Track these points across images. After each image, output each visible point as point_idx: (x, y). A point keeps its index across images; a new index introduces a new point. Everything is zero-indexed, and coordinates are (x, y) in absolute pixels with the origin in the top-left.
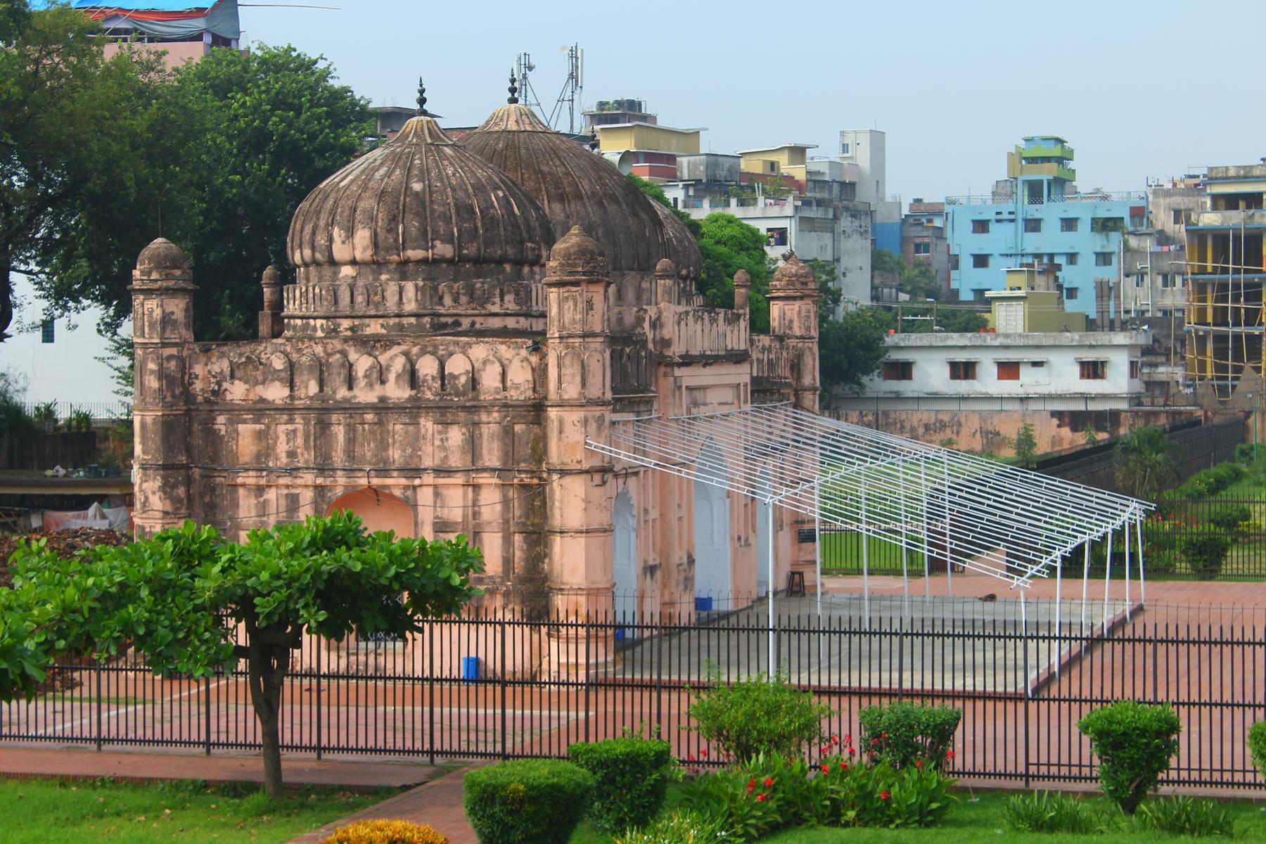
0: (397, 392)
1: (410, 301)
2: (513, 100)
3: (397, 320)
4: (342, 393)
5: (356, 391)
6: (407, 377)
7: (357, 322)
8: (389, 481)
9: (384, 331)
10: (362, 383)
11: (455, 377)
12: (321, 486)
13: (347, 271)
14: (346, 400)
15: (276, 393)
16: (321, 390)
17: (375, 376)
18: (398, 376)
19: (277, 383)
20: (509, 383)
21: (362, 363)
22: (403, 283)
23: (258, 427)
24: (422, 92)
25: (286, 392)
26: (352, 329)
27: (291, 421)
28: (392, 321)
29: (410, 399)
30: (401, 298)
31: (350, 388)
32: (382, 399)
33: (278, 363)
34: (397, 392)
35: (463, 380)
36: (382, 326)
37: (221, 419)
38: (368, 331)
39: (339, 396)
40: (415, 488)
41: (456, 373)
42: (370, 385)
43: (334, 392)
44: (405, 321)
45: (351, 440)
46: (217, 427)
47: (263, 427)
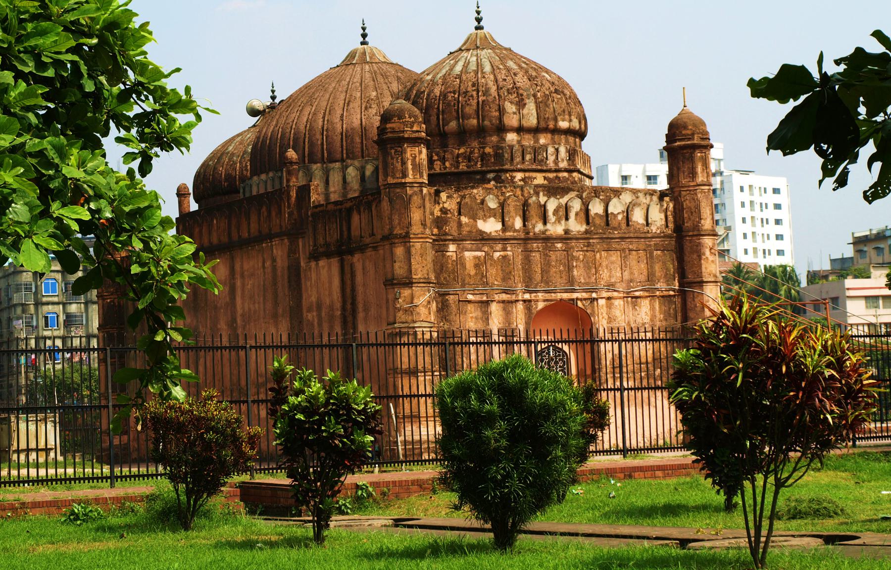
0: (576, 226)
1: (563, 160)
2: (363, 43)
3: (555, 174)
4: (539, 227)
5: (549, 226)
6: (582, 215)
7: (527, 174)
9: (546, 182)
10: (552, 218)
11: (615, 216)
12: (530, 301)
13: (511, 137)
14: (544, 232)
15: (491, 226)
16: (524, 225)
17: (562, 213)
18: (577, 214)
19: (492, 219)
20: (650, 221)
21: (552, 205)
23: (479, 254)
25: (499, 226)
26: (523, 180)
27: (504, 249)
28: (551, 175)
29: (586, 232)
31: (545, 223)
32: (567, 232)
33: (492, 204)
34: (576, 226)
35: (620, 217)
36: (545, 178)
37: (452, 247)
38: (536, 182)
39: (537, 230)
40: (593, 300)
41: (616, 213)
42: (559, 220)
43: (534, 228)
44: (561, 175)
46: (448, 254)
47: (483, 253)
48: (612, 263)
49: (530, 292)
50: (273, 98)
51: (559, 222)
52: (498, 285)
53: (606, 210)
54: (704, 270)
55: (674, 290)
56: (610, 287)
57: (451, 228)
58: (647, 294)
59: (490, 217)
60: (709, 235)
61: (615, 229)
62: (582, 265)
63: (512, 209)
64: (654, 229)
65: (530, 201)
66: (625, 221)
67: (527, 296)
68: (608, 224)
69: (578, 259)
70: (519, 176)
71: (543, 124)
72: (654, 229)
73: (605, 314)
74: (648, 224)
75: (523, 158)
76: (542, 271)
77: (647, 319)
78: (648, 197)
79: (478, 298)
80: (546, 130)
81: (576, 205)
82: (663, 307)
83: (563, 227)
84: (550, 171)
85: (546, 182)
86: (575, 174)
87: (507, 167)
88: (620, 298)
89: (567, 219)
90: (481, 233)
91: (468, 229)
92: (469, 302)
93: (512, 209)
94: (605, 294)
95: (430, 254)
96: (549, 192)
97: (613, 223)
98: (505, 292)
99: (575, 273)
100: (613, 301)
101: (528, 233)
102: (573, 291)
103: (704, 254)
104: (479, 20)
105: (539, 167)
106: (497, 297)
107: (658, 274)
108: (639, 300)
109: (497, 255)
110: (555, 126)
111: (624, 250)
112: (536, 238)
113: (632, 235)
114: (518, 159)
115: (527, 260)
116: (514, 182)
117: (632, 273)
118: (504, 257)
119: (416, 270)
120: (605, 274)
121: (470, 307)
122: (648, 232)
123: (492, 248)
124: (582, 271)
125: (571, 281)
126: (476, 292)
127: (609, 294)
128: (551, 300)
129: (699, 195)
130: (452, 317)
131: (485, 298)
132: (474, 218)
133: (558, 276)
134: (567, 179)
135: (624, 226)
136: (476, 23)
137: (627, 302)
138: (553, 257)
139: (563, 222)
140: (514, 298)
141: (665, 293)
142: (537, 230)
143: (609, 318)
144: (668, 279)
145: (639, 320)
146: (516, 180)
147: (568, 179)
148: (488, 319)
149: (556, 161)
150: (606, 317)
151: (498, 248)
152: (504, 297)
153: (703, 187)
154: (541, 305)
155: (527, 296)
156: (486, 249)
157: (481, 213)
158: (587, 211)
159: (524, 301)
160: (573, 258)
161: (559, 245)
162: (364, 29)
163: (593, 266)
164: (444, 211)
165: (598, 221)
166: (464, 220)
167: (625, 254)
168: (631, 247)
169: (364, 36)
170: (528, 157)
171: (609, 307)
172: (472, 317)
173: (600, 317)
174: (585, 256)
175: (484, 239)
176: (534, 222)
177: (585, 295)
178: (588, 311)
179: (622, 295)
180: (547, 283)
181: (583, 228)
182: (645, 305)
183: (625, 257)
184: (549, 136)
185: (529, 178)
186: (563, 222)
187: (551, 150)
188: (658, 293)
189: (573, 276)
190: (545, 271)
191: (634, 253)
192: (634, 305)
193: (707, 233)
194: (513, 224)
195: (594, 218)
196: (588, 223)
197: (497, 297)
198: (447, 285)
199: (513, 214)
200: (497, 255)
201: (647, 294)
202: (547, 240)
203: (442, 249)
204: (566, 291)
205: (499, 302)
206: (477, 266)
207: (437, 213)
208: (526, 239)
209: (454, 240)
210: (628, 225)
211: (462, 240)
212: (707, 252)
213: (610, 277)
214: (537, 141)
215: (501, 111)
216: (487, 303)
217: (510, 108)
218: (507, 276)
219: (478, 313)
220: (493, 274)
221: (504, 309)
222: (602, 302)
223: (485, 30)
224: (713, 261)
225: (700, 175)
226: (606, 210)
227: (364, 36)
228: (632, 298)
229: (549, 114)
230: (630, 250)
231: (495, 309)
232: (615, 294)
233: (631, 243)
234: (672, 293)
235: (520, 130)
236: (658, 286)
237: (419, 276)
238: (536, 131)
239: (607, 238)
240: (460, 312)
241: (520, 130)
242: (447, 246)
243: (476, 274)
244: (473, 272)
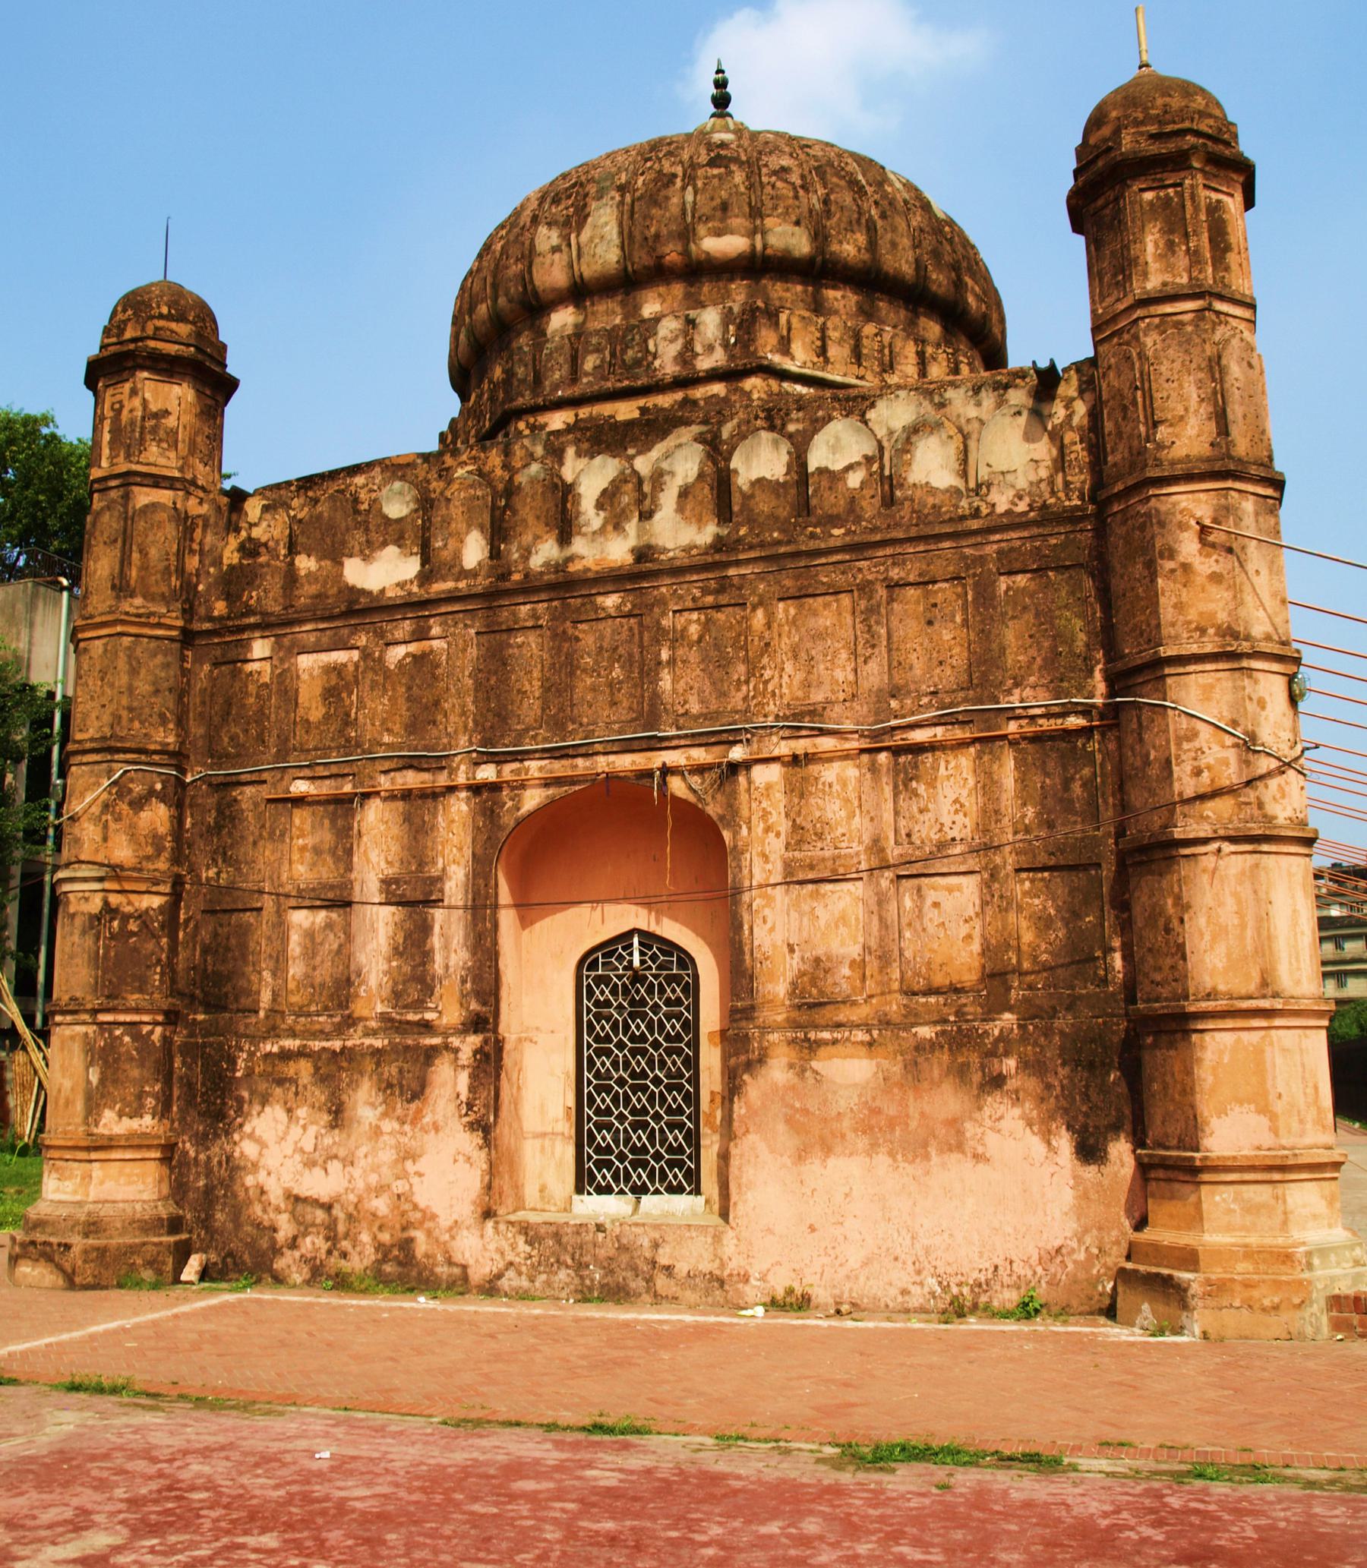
1: (710, 349)
3: (679, 396)
4: (546, 552)
6: (706, 492)
8: (659, 759)
11: (833, 477)
12: (495, 787)
14: (560, 567)
16: (495, 554)
18: (684, 493)
19: (392, 550)
22: (692, 314)
23: (340, 657)
24: (721, 84)
27: (421, 635)
29: (719, 545)
30: (689, 346)
31: (564, 538)
32: (643, 554)
34: (678, 532)
37: (260, 648)
39: (536, 562)
40: (734, 768)
41: (837, 466)
42: (616, 524)
43: (526, 554)
45: (564, 667)
47: (355, 655)
48: (819, 636)
49: (499, 759)
51: (618, 527)
52: (390, 746)
55: (1086, 711)
56: (804, 719)
57: (267, 596)
58: (959, 733)
59: (385, 544)
60: (1189, 477)
61: (834, 520)
62: (694, 656)
64: (1002, 500)
65: (521, 479)
67: (487, 773)
69: (678, 638)
71: (642, 259)
76: (546, 689)
77: (962, 827)
78: (988, 399)
79: (326, 788)
80: (658, 274)
82: (1037, 780)
83: (632, 541)
84: (658, 387)
86: (754, 384)
88: (846, 756)
89: (646, 516)
91: (312, 589)
92: (299, 801)
93: (456, 511)
94: (784, 748)
97: (829, 502)
98: (411, 764)
99: (666, 682)
100: (814, 769)
101: (504, 576)
103: (1171, 553)
106: (384, 782)
108: (928, 758)
109: (397, 653)
110: (686, 253)
112: (530, 587)
115: (496, 663)
117: (894, 665)
118: (419, 659)
119: (86, 716)
120: (785, 681)
121: (301, 818)
122: (976, 513)
123: (381, 634)
124: (693, 675)
125: (650, 712)
126: (321, 771)
127: (801, 746)
128: (571, 781)
130: (245, 850)
131: (348, 788)
132: (335, 554)
133: (603, 698)
135: (870, 507)
137: (873, 769)
140: (442, 779)
141: (1045, 724)
142: (536, 562)
143: (796, 828)
144: (1061, 671)
145: (926, 832)
148: (349, 852)
149: (686, 356)
150: (784, 826)
151: (399, 635)
152: (411, 779)
153: (1168, 309)
154: (533, 799)
156: (362, 640)
159: (476, 789)
160: (660, 635)
161: (611, 601)
164: (251, 548)
165: (764, 505)
166: (305, 564)
168: (895, 573)
170: (590, 363)
172: (303, 849)
173: (759, 828)
174: (707, 626)
175: (361, 610)
176: (527, 538)
177: (700, 755)
178: (713, 810)
179: (854, 744)
180: (558, 726)
183: (871, 611)
184: (678, 289)
186: (632, 526)
187: (669, 326)
188: (1012, 727)
189: (656, 696)
191: (911, 592)
192: (904, 782)
193: (1179, 470)
194: (457, 556)
195: (747, 497)
197: (384, 782)
198: (237, 758)
199: (458, 524)
200: (397, 653)
201: (959, 733)
202: (567, 586)
203: (232, 655)
204: (628, 747)
205: (392, 797)
207: (231, 556)
208: (498, 591)
209: (266, 626)
211: (291, 623)
212: (1188, 546)
213: (807, 685)
214: (632, 310)
216: (342, 807)
218: (423, 715)
219: (326, 836)
220: (378, 715)
221: (407, 818)
224: (1216, 578)
225: (1153, 266)
226: (798, 461)
228: (896, 751)
229: (662, 220)
230: (893, 586)
231: (377, 821)
232: (827, 743)
233: (897, 560)
234: (1074, 721)
235: (579, 292)
236: (1014, 700)
237: (91, 733)
238: (625, 283)
239: (796, 555)
240: (277, 836)
241: (579, 292)
242: (246, 645)
243: (327, 717)
244: (316, 714)
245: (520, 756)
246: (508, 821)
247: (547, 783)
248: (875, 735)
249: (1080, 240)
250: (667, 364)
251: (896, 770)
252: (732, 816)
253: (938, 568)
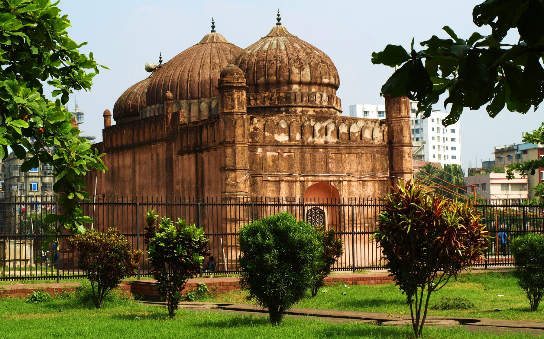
0: (331, 139)
1: (325, 101)
3: (320, 109)
4: (310, 139)
5: (316, 139)
6: (335, 133)
7: (304, 109)
8: (330, 179)
10: (317, 134)
11: (354, 134)
12: (304, 181)
13: (295, 87)
14: (313, 142)
15: (282, 138)
16: (302, 138)
17: (323, 131)
18: (332, 132)
19: (283, 134)
20: (374, 137)
21: (318, 127)
23: (275, 154)
25: (287, 138)
26: (301, 112)
27: (290, 152)
28: (318, 110)
29: (337, 143)
31: (313, 137)
32: (326, 142)
33: (283, 125)
34: (331, 139)
35: (357, 135)
36: (314, 111)
37: (260, 150)
38: (309, 113)
40: (340, 182)
41: (354, 132)
42: (321, 136)
43: (307, 139)
44: (323, 109)
46: (257, 153)
48: (352, 161)
49: (304, 176)
50: (161, 62)
51: (322, 137)
52: (285, 172)
53: (349, 130)
54: (404, 166)
55: (387, 177)
56: (350, 174)
57: (259, 139)
58: (371, 179)
59: (282, 133)
61: (354, 141)
62: (334, 162)
63: (294, 128)
64: (376, 142)
65: (305, 124)
66: (359, 137)
67: (302, 179)
68: (349, 138)
69: (332, 158)
70: (299, 110)
71: (314, 80)
72: (376, 142)
73: (346, 190)
74: (373, 139)
75: (302, 100)
76: (311, 165)
77: (371, 194)
78: (373, 124)
79: (274, 179)
80: (316, 84)
81: (332, 127)
82: (380, 187)
83: (324, 140)
84: (317, 107)
85: (315, 113)
86: (332, 109)
87: (292, 104)
89: (326, 135)
90: (277, 142)
91: (269, 139)
92: (269, 181)
93: (294, 128)
94: (347, 179)
95: (247, 153)
96: (316, 119)
97: (353, 138)
98: (290, 176)
99: (330, 166)
100: (352, 182)
101: (303, 143)
102: (329, 176)
103: (405, 157)
104: (279, 20)
105: (311, 105)
107: (378, 168)
108: (366, 182)
110: (321, 81)
111: (358, 153)
112: (308, 146)
113: (363, 145)
114: (299, 100)
115: (303, 158)
116: (296, 113)
117: (363, 167)
118: (289, 156)
119: (239, 162)
120: (347, 167)
121: (269, 184)
124: (334, 165)
125: (328, 170)
126: (273, 176)
128: (316, 181)
129: (403, 123)
130: (259, 190)
131: (278, 179)
132: (273, 133)
133: (320, 167)
134: (326, 112)
135: (359, 140)
136: (277, 22)
138: (318, 157)
139: (324, 137)
140: (294, 179)
141: (382, 179)
143: (349, 192)
144: (384, 171)
145: (366, 194)
146: (298, 112)
147: (327, 112)
148: (279, 191)
150: (347, 192)
151: (286, 151)
152: (289, 179)
154: (310, 184)
155: (302, 179)
156: (279, 151)
157: (277, 130)
158: (338, 131)
159: (301, 181)
160: (329, 157)
161: (321, 150)
162: (213, 23)
163: (340, 162)
164: (255, 129)
165: (344, 137)
166: (267, 134)
167: (359, 156)
169: (213, 27)
170: (305, 99)
171: (349, 186)
172: (270, 190)
173: (344, 192)
174: (336, 156)
175: (278, 145)
176: (307, 136)
177: (335, 179)
178: (337, 188)
179: (357, 179)
180: (314, 171)
181: (335, 140)
182: (370, 185)
183: (359, 157)
184: (317, 87)
185: (305, 111)
186: (324, 137)
187: (318, 95)
188: (377, 179)
189: (329, 168)
190: (312, 165)
191: (364, 155)
192: (364, 185)
194: (295, 137)
195: (341, 135)
196: (338, 138)
197: (284, 179)
198: (256, 171)
199: (295, 131)
200: (285, 155)
201: (371, 179)
202: (315, 146)
203: (254, 150)
204: (325, 176)
205: (286, 182)
206: (274, 161)
207: (251, 130)
208: (303, 146)
209: (261, 146)
210: (361, 139)
211: (266, 146)
212: (407, 156)
213: (350, 169)
214: (310, 90)
215: (290, 72)
216: (279, 182)
217: (295, 70)
219: (274, 188)
220: (283, 166)
221: (289, 186)
222: (345, 183)
223: (282, 26)
224: (409, 161)
226: (349, 130)
227: (213, 27)
228: (363, 181)
229: (317, 74)
230: (362, 154)
232: (353, 179)
234: (385, 179)
235: (300, 83)
236: (378, 175)
237: (240, 166)
239: (349, 146)
240: (263, 187)
241: (300, 83)
242: (257, 149)
243: (273, 165)
244: (271, 164)
245: (307, 176)
246: (306, 188)
247: (312, 181)
248: (360, 178)
249: (383, 99)
250: (318, 103)
251: (363, 184)
252: (340, 189)
253: (368, 152)
